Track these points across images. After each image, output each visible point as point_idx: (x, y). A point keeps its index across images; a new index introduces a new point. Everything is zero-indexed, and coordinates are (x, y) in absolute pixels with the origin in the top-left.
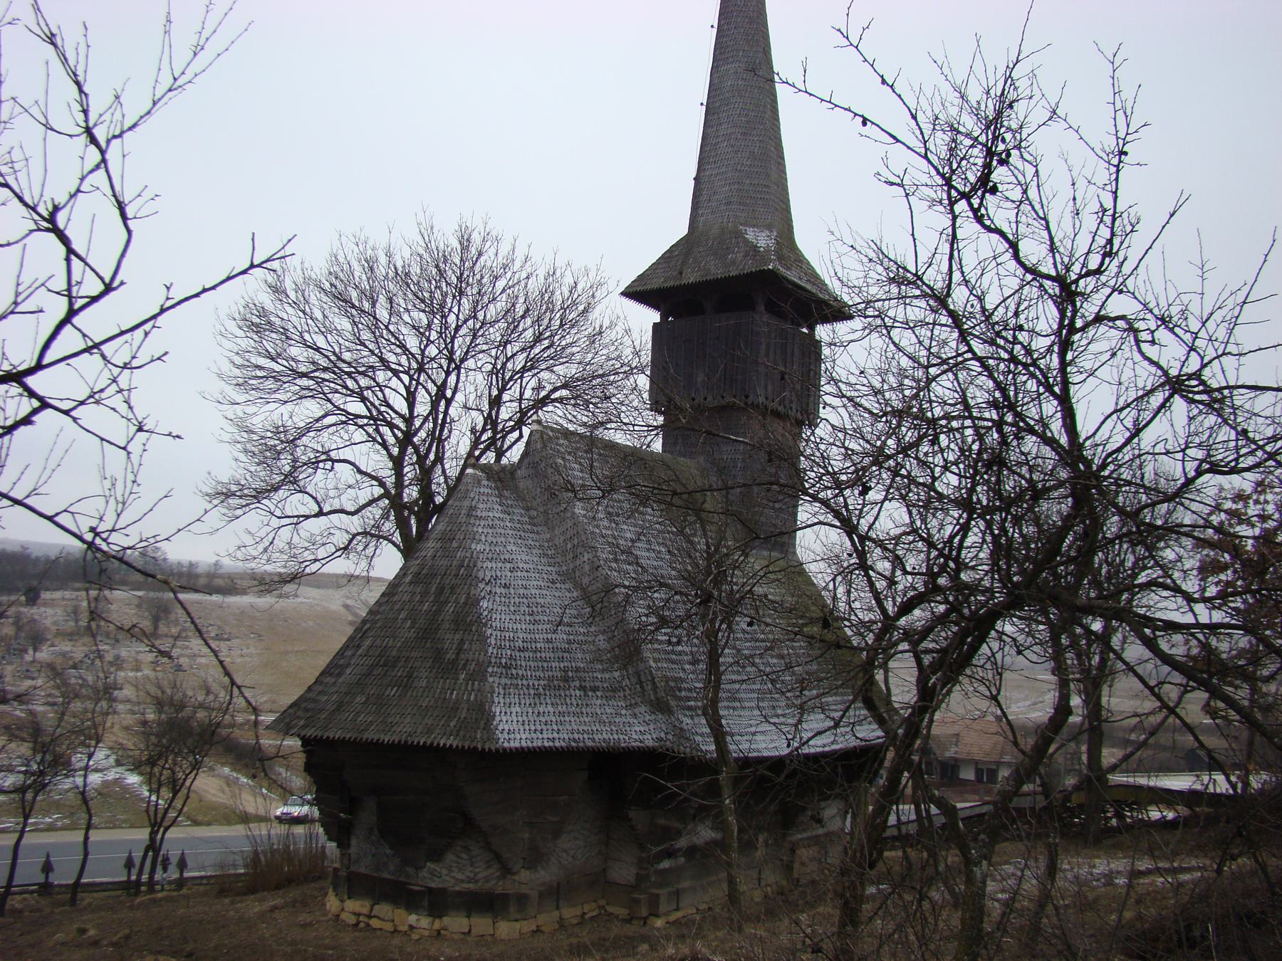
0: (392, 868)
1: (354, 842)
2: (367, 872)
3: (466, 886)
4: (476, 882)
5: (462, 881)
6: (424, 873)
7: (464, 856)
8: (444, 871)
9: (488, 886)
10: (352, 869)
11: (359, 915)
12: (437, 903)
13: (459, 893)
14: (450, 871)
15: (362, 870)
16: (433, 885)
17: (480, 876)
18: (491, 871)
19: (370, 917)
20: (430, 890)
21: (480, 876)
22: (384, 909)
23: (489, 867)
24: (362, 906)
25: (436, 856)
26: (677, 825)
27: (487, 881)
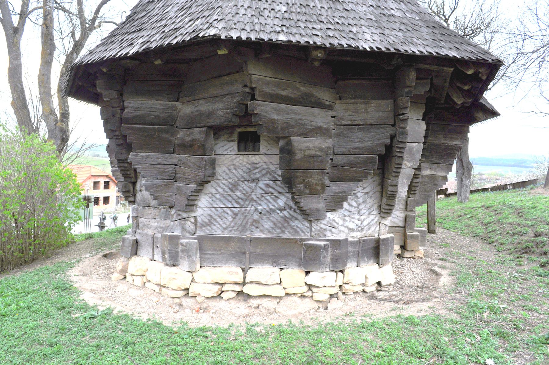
0: (267, 225)
1: (203, 201)
2: (226, 234)
3: (355, 234)
4: (362, 229)
5: (353, 230)
6: (323, 224)
7: (355, 204)
8: (341, 222)
9: (369, 232)
10: (199, 233)
11: (222, 284)
12: (339, 255)
13: (353, 244)
14: (344, 220)
15: (218, 233)
16: (332, 238)
17: (365, 223)
18: (372, 217)
19: (244, 284)
20: (336, 243)
21: (365, 223)
22: (262, 272)
23: (369, 214)
24: (231, 273)
25: (336, 204)
26: (442, 174)
27: (369, 229)
